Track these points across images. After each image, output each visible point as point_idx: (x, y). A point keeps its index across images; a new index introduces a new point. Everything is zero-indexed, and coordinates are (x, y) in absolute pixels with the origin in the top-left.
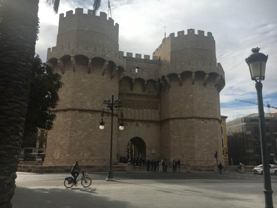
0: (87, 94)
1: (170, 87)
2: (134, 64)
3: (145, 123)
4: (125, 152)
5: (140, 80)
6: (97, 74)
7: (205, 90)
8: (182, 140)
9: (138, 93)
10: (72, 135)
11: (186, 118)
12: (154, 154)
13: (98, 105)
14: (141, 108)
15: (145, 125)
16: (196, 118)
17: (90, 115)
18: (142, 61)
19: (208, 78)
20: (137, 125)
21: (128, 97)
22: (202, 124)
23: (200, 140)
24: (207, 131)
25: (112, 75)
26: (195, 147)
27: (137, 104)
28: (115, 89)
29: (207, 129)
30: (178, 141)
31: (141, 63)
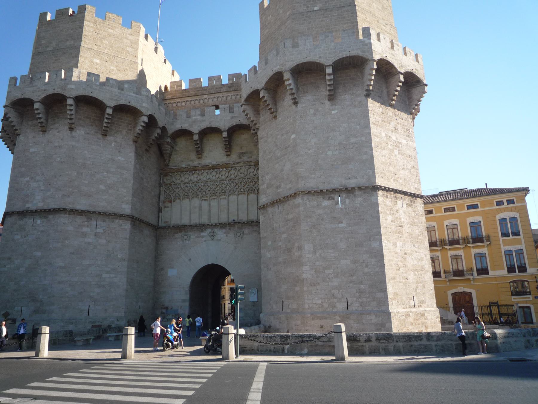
0: (38, 178)
1: (258, 129)
3: (229, 229)
4: (184, 301)
5: (209, 132)
6: (58, 132)
7: (333, 112)
8: (280, 260)
11: (284, 198)
13: (57, 196)
16: (303, 193)
17: (39, 221)
19: (332, 77)
20: (213, 236)
21: (193, 174)
22: (325, 207)
24: (343, 227)
25: (104, 128)
26: (304, 276)
28: (120, 158)
29: (342, 223)
31: (221, 95)
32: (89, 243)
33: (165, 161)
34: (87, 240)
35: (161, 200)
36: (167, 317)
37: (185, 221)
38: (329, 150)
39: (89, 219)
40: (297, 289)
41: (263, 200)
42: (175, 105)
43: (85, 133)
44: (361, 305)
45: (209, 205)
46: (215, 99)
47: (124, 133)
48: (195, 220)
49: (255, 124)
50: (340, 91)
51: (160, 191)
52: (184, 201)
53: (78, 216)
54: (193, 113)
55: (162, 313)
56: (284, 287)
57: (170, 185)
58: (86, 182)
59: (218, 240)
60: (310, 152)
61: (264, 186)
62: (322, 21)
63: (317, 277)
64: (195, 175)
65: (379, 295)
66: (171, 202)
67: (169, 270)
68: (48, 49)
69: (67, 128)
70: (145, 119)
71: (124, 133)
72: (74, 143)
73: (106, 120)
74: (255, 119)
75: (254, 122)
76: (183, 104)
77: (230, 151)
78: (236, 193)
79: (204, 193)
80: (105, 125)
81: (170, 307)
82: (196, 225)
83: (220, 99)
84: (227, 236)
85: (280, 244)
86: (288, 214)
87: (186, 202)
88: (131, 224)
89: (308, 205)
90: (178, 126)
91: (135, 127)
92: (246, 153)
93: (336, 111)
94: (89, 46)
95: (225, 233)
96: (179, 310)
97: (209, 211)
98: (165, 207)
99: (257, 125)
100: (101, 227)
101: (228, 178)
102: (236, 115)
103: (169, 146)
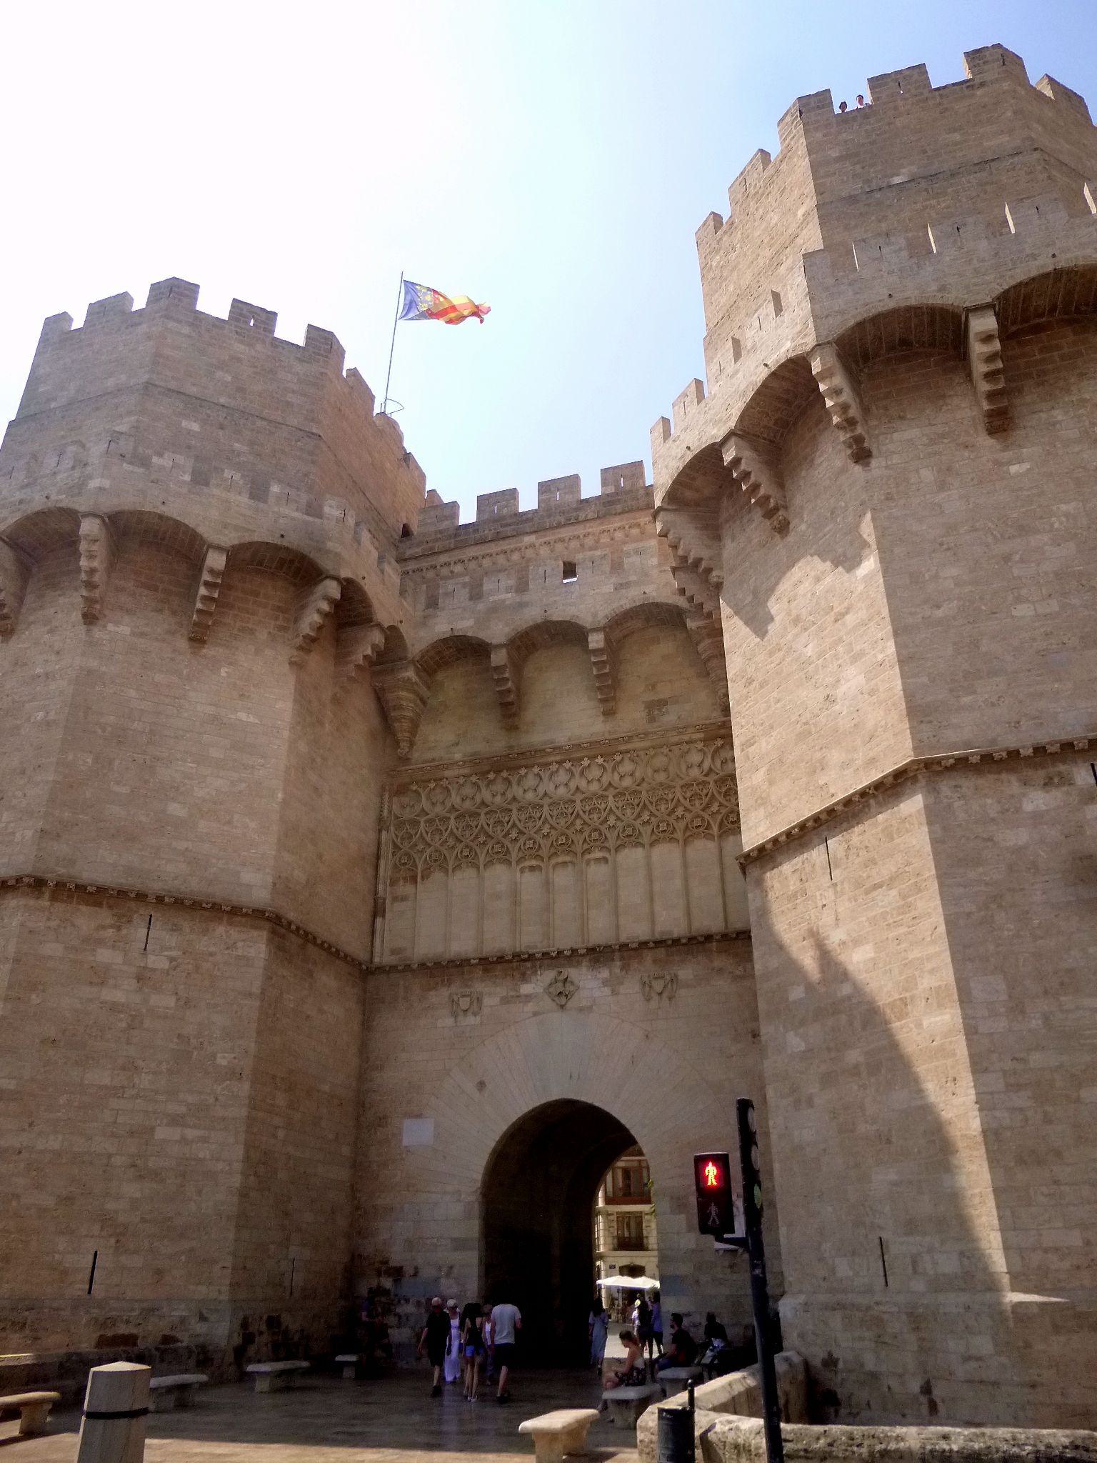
1: (719, 586)
2: (530, 553)
4: (459, 1244)
8: (854, 1056)
11: (848, 802)
13: (18, 837)
14: (588, 851)
15: (631, 987)
18: (582, 516)
20: (562, 994)
21: (491, 782)
22: (1037, 817)
23: (1046, 1018)
27: (562, 821)
28: (243, 716)
30: (827, 1080)
31: (580, 530)
32: (114, 1008)
33: (397, 744)
34: (108, 995)
36: (399, 1310)
37: (463, 945)
38: (1019, 600)
41: (756, 830)
42: (430, 574)
43: (133, 634)
45: (548, 884)
46: (559, 547)
47: (262, 635)
48: (498, 939)
49: (708, 571)
52: (459, 874)
53: (84, 908)
54: (488, 586)
56: (883, 1177)
57: (415, 823)
58: (125, 790)
59: (581, 1010)
60: (939, 613)
61: (759, 777)
63: (1048, 1120)
64: (499, 787)
66: (414, 879)
67: (408, 1123)
69: (76, 616)
70: (333, 589)
71: (262, 635)
72: (93, 664)
73: (203, 591)
74: (705, 553)
76: (458, 568)
77: (614, 698)
78: (646, 839)
79: (530, 844)
80: (199, 605)
81: (409, 1270)
82: (501, 959)
84: (614, 993)
88: (270, 941)
89: (962, 816)
90: (442, 626)
91: (296, 621)
95: (605, 983)
96: (443, 1281)
97: (548, 908)
98: (395, 899)
99: (714, 573)
100: (163, 949)
101: (611, 792)
103: (411, 696)
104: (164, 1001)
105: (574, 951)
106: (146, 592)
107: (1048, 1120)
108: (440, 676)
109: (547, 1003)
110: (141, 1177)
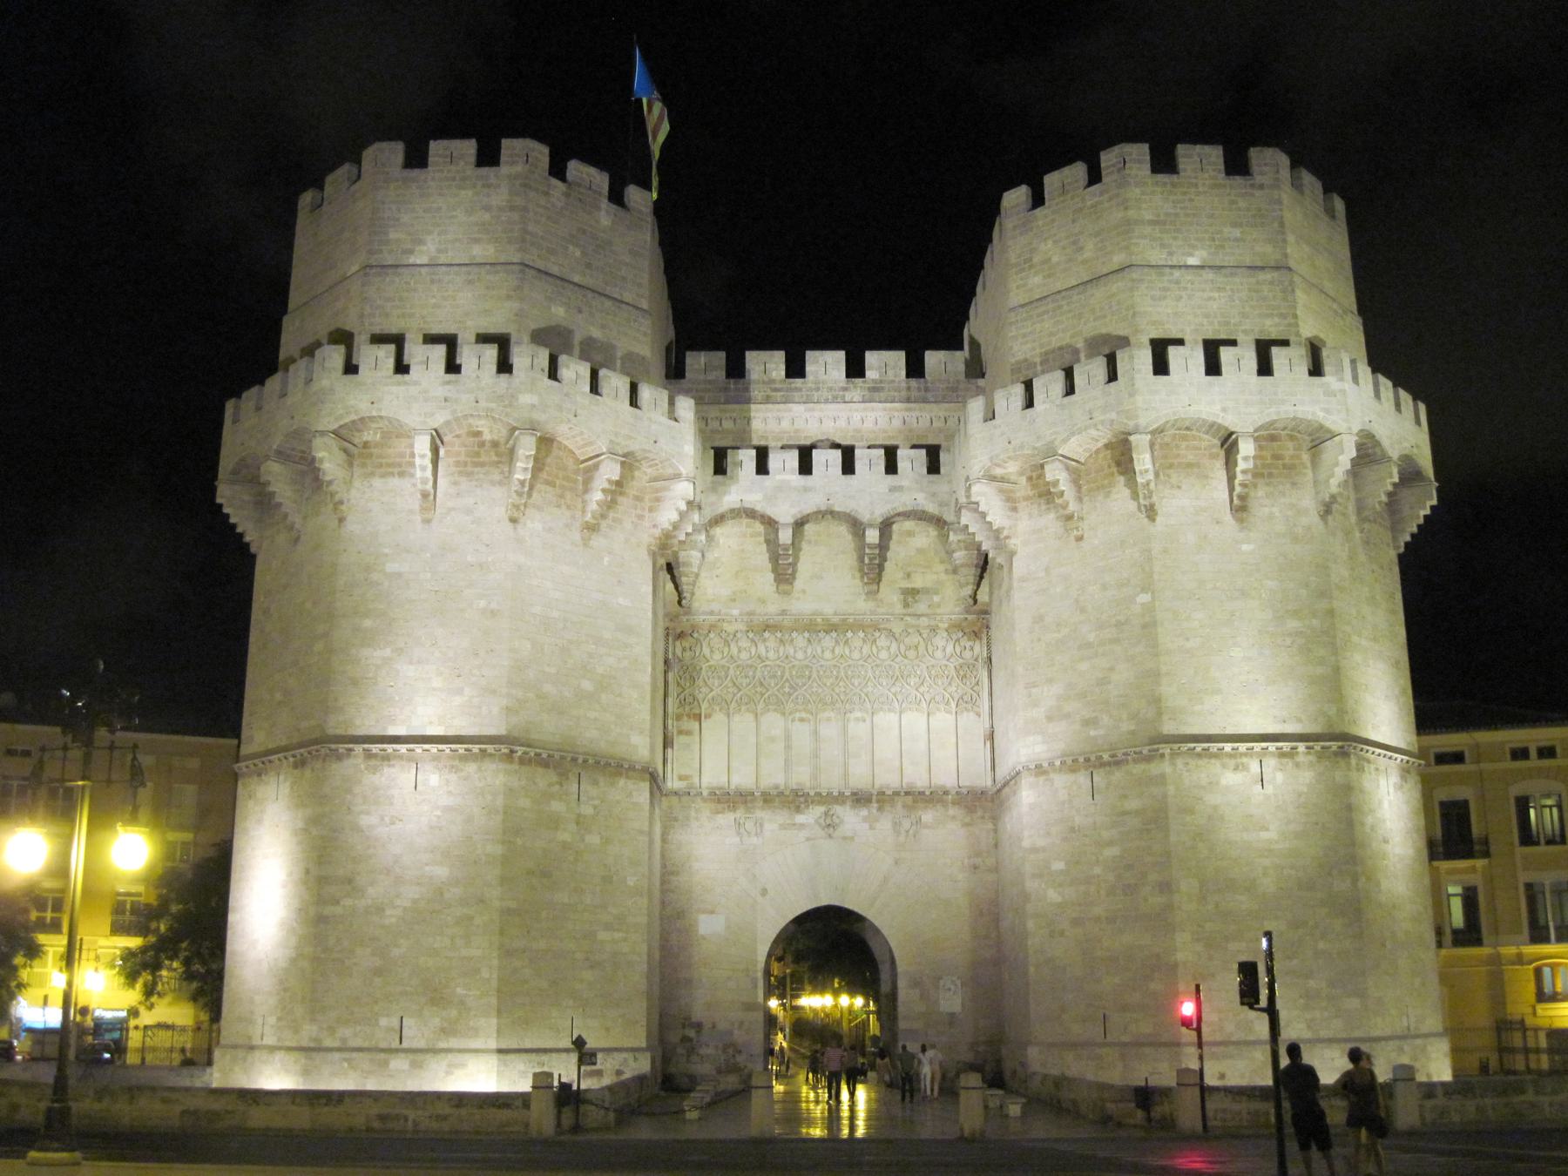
2: (799, 424)
3: (880, 809)
7: (1245, 547)
8: (1098, 911)
9: (828, 610)
10: (329, 910)
12: (952, 1015)
23: (1217, 906)
26: (1180, 956)
28: (621, 600)
32: (565, 846)
35: (670, 710)
39: (563, 775)
40: (1154, 986)
44: (1309, 1027)
48: (773, 776)
49: (1007, 537)
50: (1260, 493)
51: (666, 682)
52: (737, 718)
54: (774, 461)
55: (685, 1039)
58: (553, 670)
59: (845, 838)
60: (1189, 645)
62: (1210, 299)
63: (1211, 958)
65: (1353, 1003)
66: (698, 718)
68: (411, 261)
69: (501, 512)
75: (1005, 533)
83: (842, 423)
84: (871, 828)
85: (1097, 870)
86: (1125, 797)
87: (743, 722)
92: (926, 591)
93: (1251, 547)
94: (540, 264)
95: (865, 819)
97: (816, 755)
98: (680, 732)
102: (905, 483)
104: (594, 839)
105: (841, 794)
106: (549, 489)
107: (1211, 958)
108: (718, 531)
109: (821, 833)
110: (592, 967)
